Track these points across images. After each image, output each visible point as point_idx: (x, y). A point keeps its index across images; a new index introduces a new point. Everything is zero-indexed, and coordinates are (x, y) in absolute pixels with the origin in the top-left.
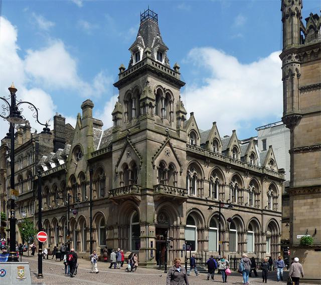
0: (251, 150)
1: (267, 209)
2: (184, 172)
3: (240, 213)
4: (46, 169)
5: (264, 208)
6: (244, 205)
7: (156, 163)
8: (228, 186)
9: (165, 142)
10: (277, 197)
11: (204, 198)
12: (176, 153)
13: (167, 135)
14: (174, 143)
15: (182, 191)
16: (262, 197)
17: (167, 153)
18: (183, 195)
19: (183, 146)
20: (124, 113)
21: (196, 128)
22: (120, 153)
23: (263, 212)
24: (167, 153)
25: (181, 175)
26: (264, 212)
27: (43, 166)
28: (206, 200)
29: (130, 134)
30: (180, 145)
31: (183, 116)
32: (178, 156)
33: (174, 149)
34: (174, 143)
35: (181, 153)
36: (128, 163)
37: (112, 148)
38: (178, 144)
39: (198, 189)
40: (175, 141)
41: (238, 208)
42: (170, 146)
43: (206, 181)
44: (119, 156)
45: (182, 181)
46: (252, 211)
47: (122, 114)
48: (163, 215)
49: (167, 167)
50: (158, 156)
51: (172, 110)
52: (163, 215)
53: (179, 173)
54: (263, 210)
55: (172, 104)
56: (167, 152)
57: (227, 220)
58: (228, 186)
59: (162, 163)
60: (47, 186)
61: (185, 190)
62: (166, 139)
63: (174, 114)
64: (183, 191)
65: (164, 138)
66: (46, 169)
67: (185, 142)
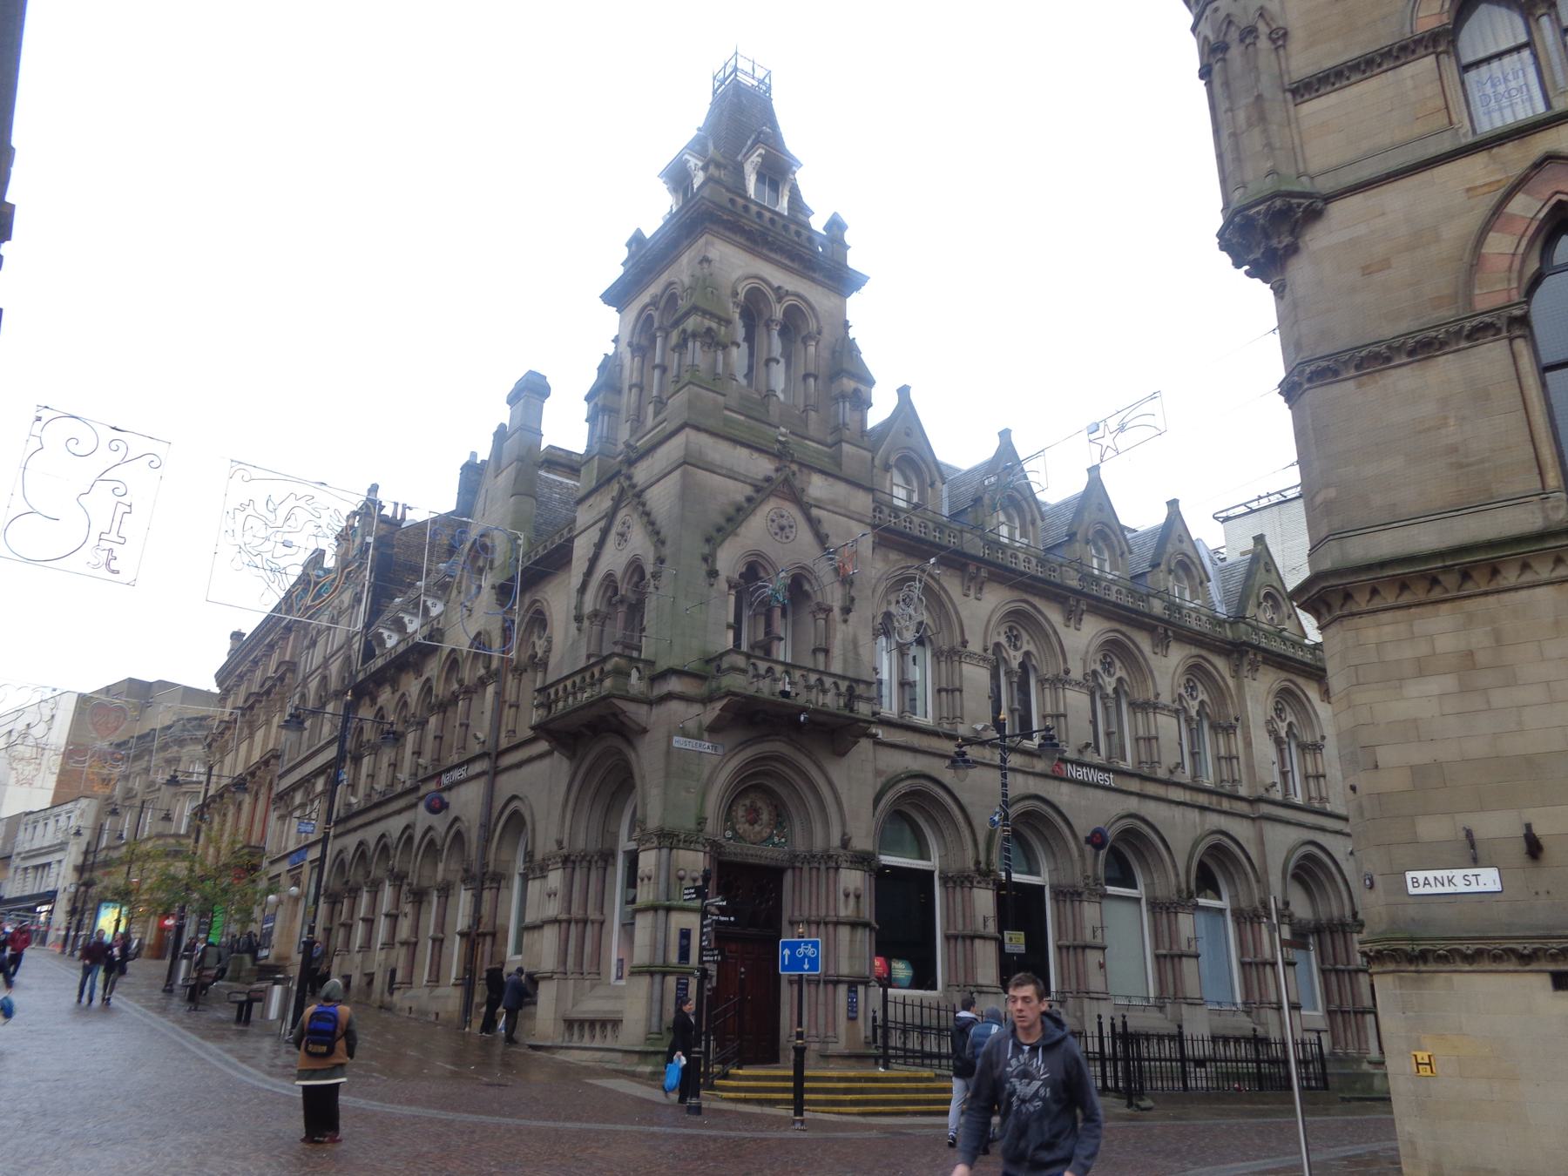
1: (1277, 795)
3: (1151, 810)
5: (1261, 792)
7: (729, 559)
8: (1078, 684)
9: (768, 479)
10: (1316, 748)
12: (826, 528)
13: (781, 454)
14: (818, 486)
15: (843, 686)
16: (1248, 744)
18: (849, 706)
19: (861, 502)
22: (594, 535)
23: (1260, 808)
24: (782, 528)
25: (845, 621)
26: (1266, 809)
31: (856, 391)
34: (818, 486)
36: (619, 574)
39: (939, 691)
41: (1134, 785)
42: (796, 497)
43: (971, 655)
50: (734, 533)
51: (812, 369)
54: (1260, 800)
55: (812, 349)
57: (1089, 840)
58: (1078, 684)
59: (753, 571)
62: (777, 470)
63: (820, 382)
64: (850, 689)
65: (763, 466)
67: (870, 490)
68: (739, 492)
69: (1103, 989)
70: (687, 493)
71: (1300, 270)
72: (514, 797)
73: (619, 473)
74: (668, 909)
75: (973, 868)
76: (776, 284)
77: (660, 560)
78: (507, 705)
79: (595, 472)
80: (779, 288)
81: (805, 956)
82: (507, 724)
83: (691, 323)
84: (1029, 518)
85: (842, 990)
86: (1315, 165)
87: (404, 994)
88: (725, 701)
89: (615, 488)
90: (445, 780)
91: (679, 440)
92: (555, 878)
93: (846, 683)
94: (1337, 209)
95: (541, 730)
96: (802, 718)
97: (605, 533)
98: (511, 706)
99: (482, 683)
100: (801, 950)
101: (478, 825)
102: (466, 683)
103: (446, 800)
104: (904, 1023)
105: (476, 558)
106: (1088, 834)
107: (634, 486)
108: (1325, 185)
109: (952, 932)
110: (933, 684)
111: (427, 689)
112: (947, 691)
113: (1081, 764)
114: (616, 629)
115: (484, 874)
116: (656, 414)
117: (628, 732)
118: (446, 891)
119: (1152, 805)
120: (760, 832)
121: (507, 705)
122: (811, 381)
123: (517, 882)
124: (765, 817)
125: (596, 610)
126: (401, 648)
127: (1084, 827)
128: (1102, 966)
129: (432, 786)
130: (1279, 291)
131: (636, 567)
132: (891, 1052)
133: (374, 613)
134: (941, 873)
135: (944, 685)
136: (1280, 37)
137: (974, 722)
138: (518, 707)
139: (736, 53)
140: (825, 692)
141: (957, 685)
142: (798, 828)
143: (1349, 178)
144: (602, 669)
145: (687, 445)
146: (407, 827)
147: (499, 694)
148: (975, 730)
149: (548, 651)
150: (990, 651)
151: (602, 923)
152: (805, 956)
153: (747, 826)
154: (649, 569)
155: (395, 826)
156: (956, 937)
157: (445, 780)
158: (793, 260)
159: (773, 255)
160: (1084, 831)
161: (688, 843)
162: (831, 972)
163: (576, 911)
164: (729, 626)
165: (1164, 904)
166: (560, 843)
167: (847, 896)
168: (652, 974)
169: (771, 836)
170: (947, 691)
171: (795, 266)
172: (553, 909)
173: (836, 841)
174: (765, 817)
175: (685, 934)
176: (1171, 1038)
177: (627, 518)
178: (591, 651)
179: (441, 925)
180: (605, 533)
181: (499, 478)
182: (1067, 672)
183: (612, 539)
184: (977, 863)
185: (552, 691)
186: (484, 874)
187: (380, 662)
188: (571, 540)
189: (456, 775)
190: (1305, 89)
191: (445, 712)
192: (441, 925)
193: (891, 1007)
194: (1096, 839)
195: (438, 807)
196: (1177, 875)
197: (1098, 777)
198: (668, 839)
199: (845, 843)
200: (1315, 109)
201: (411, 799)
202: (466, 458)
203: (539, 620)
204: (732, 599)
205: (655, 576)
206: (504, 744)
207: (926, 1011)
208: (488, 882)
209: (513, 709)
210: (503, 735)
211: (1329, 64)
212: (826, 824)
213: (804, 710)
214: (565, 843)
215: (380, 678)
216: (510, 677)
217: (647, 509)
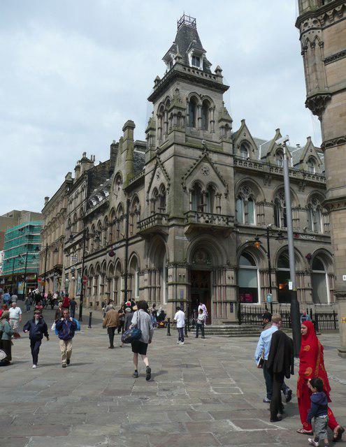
2: (232, 194)
4: (95, 203)
7: (189, 185)
8: (303, 209)
12: (219, 170)
14: (214, 157)
18: (227, 223)
19: (230, 160)
32: (221, 173)
34: (214, 157)
42: (209, 161)
49: (204, 189)
53: (223, 196)
56: (204, 170)
57: (306, 257)
59: (197, 185)
65: (199, 153)
68: (191, 162)
70: (176, 165)
71: (326, 115)
72: (134, 252)
73: (156, 157)
74: (177, 284)
77: (169, 185)
83: (174, 111)
85: (228, 305)
86: (329, 84)
89: (154, 162)
90: (114, 247)
91: (173, 147)
92: (146, 276)
94: (334, 98)
95: (138, 234)
97: (153, 175)
99: (122, 218)
105: (117, 180)
108: (332, 90)
111: (106, 218)
113: (303, 234)
114: (158, 204)
116: (166, 138)
117: (165, 236)
118: (117, 279)
122: (212, 123)
123: (136, 275)
124: (204, 257)
126: (98, 206)
127: (305, 253)
129: (110, 249)
130: (321, 119)
131: (162, 185)
133: (89, 194)
136: (322, 44)
141: (262, 213)
142: (214, 258)
143: (337, 89)
146: (104, 260)
147: (127, 222)
149: (140, 209)
151: (160, 288)
154: (166, 187)
155: (101, 259)
157: (114, 247)
160: (305, 255)
161: (182, 266)
163: (153, 285)
166: (147, 266)
168: (173, 302)
169: (206, 262)
172: (146, 284)
173: (225, 262)
174: (204, 257)
175: (182, 291)
176: (330, 315)
179: (116, 288)
180: (153, 175)
182: (299, 206)
183: (155, 177)
187: (92, 210)
188: (144, 176)
189: (117, 245)
190: (328, 61)
192: (116, 288)
194: (309, 257)
195: (112, 254)
197: (310, 238)
198: (176, 265)
199: (228, 264)
200: (331, 66)
201: (105, 252)
202: (112, 142)
203: (137, 200)
205: (168, 189)
206: (130, 236)
210: (129, 234)
211: (334, 53)
212: (222, 257)
215: (93, 216)
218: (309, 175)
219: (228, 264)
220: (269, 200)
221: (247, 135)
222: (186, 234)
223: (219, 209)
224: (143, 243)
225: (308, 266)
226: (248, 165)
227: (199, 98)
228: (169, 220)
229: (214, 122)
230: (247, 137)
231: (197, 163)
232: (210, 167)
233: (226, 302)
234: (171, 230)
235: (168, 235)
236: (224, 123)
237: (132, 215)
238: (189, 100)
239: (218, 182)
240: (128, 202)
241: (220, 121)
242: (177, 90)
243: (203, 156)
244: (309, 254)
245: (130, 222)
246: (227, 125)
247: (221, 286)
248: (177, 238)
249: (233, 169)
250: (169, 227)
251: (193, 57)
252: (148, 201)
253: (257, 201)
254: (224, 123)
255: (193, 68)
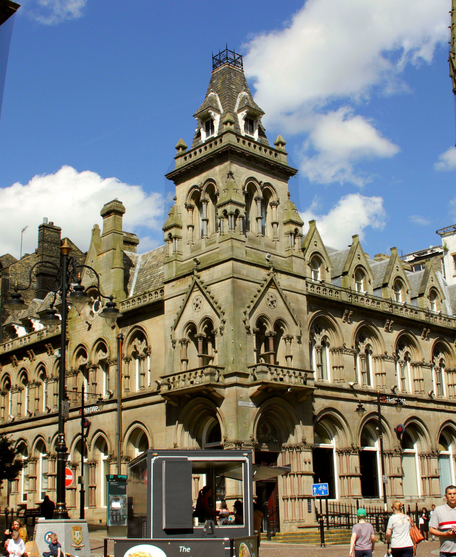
0: (430, 284)
3: (420, 414)
4: (21, 331)
6: (426, 397)
8: (390, 358)
11: (345, 386)
12: (289, 300)
15: (303, 374)
17: (272, 302)
18: (305, 383)
19: (300, 285)
20: (185, 227)
21: (323, 250)
22: (179, 301)
24: (272, 302)
27: (16, 327)
28: (352, 390)
29: (200, 267)
30: (293, 284)
32: (293, 305)
33: (284, 292)
34: (282, 280)
35: (297, 300)
36: (197, 323)
37: (162, 291)
38: (289, 283)
40: (283, 276)
41: (414, 404)
44: (179, 310)
45: (301, 353)
46: (442, 407)
47: (181, 228)
48: (268, 426)
49: (270, 329)
52: (268, 426)
53: (295, 340)
56: (271, 299)
58: (390, 358)
60: (23, 368)
61: (308, 372)
65: (263, 273)
66: (21, 331)
67: (304, 278)
69: (402, 494)
75: (351, 446)
76: (259, 181)
78: (123, 377)
79: (174, 269)
80: (261, 182)
81: (322, 489)
82: (124, 385)
83: (230, 208)
84: (368, 280)
87: (74, 512)
88: (260, 386)
89: (189, 281)
93: (304, 373)
96: (289, 390)
98: (126, 377)
100: (321, 487)
101: (115, 434)
102: (93, 363)
103: (90, 421)
104: (334, 512)
106: (396, 427)
107: (202, 283)
109: (342, 474)
110: (330, 364)
112: (337, 367)
115: (122, 457)
117: (219, 401)
119: (421, 411)
120: (268, 437)
121: (123, 377)
122: (275, 225)
124: (269, 431)
125: (184, 339)
128: (401, 484)
132: (330, 525)
134: (336, 449)
135: (335, 365)
137: (349, 381)
138: (129, 377)
139: (227, 49)
140: (290, 376)
141: (341, 365)
144: (202, 371)
145: (233, 268)
147: (119, 371)
148: (351, 386)
150: (354, 347)
152: (322, 489)
153: (263, 436)
154: (217, 324)
156: (344, 477)
158: (265, 166)
159: (259, 165)
160: (394, 426)
162: (300, 494)
164: (255, 351)
165: (425, 455)
167: (306, 463)
169: (272, 440)
170: (337, 367)
171: (266, 168)
173: (300, 441)
174: (269, 431)
177: (199, 297)
178: (182, 358)
181: (101, 256)
184: (352, 445)
185: (171, 378)
186: (122, 457)
187: (18, 344)
191: (77, 376)
193: (329, 506)
194: (398, 431)
196: (431, 442)
202: (41, 223)
204: (254, 337)
205: (222, 329)
206: (124, 395)
207: (347, 508)
208: (124, 460)
209: (127, 378)
210: (123, 390)
213: (289, 387)
214: (178, 445)
216: (123, 362)
217: (211, 294)
218: (357, 296)
219: (305, 443)
220: (348, 346)
221: (319, 244)
222: (253, 398)
223: (289, 359)
224: (163, 405)
225: (397, 443)
226: (321, 291)
227: (258, 186)
228: (226, 376)
229: (277, 224)
230: (319, 249)
231: (262, 289)
232: (278, 295)
233: (303, 498)
234: (226, 392)
235: (223, 398)
236: (292, 228)
237: (128, 360)
238: (246, 190)
239: (288, 318)
240: (120, 340)
241: (285, 224)
242: (230, 174)
243: (269, 279)
244: (399, 427)
245: (124, 372)
246: (296, 230)
247: (294, 475)
248: (240, 403)
249: (305, 297)
250: (225, 387)
251: (246, 119)
252: (174, 342)
253: (332, 345)
254: (292, 228)
255: (246, 138)
